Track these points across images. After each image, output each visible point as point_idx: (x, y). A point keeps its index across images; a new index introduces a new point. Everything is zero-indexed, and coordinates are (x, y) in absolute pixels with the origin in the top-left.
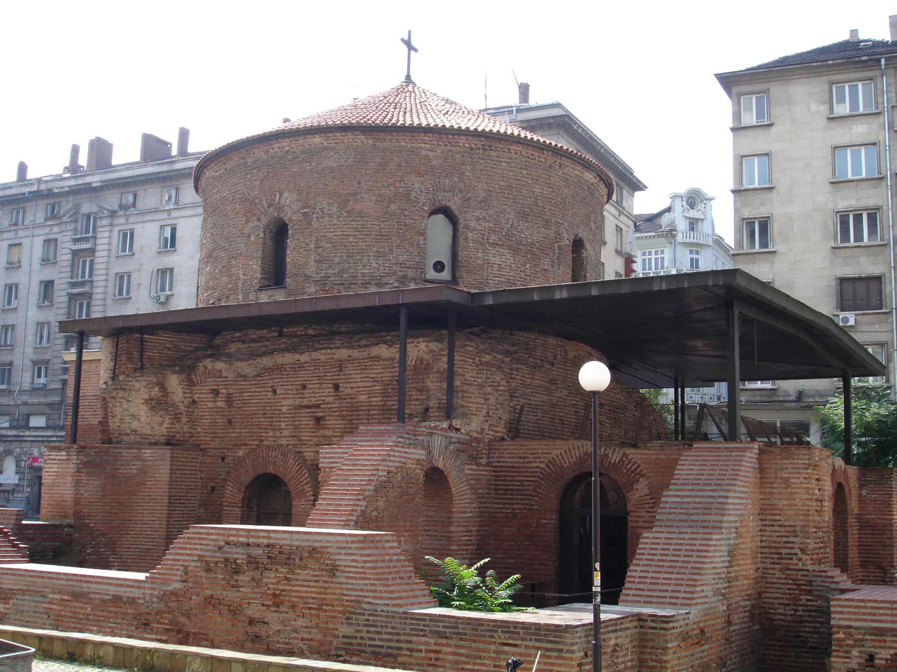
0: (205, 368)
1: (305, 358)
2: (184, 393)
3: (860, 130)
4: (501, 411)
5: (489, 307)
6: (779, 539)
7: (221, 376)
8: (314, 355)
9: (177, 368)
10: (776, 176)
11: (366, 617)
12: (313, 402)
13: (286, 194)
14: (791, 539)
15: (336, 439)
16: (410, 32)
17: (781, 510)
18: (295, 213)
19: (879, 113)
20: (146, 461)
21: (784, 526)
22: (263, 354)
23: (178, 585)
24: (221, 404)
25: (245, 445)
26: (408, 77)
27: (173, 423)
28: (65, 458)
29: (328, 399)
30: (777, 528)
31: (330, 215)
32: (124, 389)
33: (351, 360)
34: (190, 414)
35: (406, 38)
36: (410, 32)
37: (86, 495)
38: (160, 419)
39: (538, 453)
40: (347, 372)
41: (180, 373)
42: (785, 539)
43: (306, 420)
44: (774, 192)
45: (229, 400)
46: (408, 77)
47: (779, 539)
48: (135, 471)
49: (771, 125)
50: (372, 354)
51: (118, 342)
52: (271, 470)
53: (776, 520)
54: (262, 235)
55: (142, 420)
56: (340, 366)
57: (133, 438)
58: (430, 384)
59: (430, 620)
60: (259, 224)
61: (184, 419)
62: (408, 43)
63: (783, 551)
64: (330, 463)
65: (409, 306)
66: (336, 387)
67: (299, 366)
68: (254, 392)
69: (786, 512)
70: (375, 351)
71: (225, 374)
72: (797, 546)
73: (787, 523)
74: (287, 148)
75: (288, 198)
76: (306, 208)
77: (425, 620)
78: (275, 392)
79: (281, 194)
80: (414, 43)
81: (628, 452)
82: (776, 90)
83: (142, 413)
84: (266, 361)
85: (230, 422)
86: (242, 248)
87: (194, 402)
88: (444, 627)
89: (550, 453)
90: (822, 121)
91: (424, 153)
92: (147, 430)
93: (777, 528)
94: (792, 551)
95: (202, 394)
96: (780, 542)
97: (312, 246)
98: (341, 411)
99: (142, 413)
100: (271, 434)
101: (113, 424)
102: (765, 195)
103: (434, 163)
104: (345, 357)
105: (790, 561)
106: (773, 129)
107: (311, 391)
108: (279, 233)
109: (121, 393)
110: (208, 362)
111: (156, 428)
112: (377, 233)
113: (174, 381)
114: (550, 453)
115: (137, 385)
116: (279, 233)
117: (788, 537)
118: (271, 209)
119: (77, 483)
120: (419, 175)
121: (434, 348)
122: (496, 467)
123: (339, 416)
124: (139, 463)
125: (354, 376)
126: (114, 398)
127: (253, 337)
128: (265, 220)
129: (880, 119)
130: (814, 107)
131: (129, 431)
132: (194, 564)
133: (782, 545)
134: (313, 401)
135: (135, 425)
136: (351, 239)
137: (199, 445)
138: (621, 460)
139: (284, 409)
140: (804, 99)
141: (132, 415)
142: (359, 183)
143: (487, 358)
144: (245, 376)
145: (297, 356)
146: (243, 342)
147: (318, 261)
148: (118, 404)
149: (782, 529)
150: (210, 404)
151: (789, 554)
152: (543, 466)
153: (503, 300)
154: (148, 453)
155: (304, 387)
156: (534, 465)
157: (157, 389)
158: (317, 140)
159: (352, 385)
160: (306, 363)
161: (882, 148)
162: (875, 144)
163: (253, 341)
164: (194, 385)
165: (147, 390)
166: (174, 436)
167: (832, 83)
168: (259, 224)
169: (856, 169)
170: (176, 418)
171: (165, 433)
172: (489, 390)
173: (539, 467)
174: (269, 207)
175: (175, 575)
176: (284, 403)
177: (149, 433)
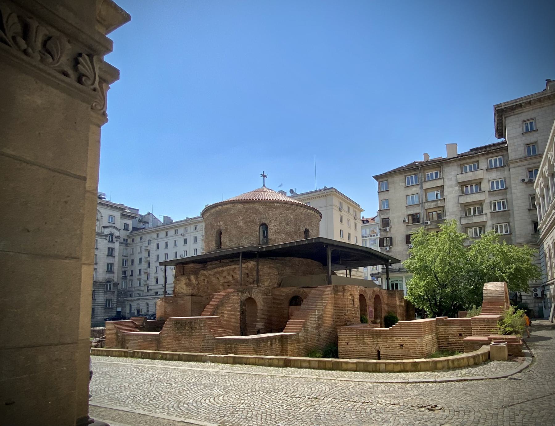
1: (224, 269)
33: (235, 268)
66: (233, 276)
67: (223, 271)
82: (390, 180)
84: (215, 270)
102: (388, 211)
129: (419, 186)
130: (401, 184)
140: (399, 181)
153: (268, 249)
167: (405, 176)
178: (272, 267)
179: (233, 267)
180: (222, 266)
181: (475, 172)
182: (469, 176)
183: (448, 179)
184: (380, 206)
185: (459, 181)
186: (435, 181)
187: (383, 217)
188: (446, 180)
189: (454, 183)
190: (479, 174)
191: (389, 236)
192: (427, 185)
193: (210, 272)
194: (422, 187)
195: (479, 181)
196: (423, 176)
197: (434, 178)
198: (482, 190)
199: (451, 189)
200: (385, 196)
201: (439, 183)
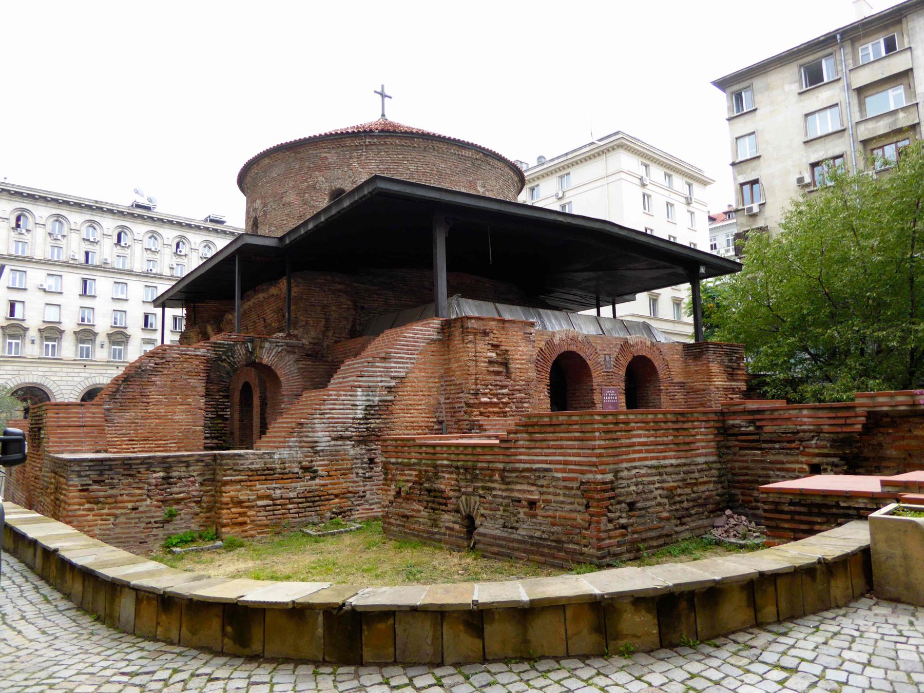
4: (345, 322)
16: (383, 86)
19: (839, 79)
26: (383, 115)
30: (452, 387)
35: (379, 90)
36: (383, 86)
41: (212, 325)
44: (761, 159)
46: (383, 115)
49: (755, 110)
62: (383, 95)
66: (265, 320)
80: (387, 92)
90: (794, 97)
91: (324, 155)
94: (460, 405)
103: (330, 160)
106: (757, 112)
120: (320, 170)
129: (841, 84)
130: (787, 87)
143: (339, 287)
161: (844, 106)
162: (837, 105)
172: (334, 308)
178: (340, 291)
186: (885, 62)
187: (742, 180)
188: (918, 52)
191: (760, 223)
192: (863, 78)
194: (849, 86)
196: (850, 56)
197: (883, 54)
200: (744, 126)
201: (897, 64)
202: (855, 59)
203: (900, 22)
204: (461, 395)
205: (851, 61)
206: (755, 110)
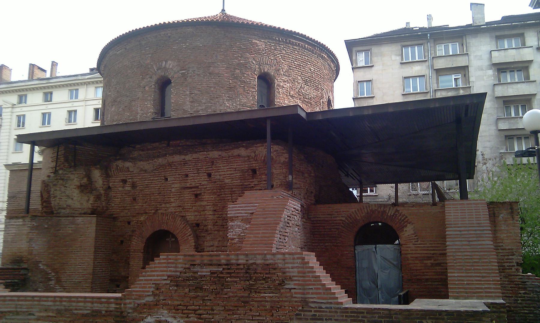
0: (117, 166)
1: (188, 157)
2: (103, 182)
3: (417, 69)
5: (320, 121)
6: (503, 257)
7: (129, 171)
8: (195, 156)
9: (98, 166)
10: (375, 91)
11: (313, 313)
12: (193, 185)
13: (169, 62)
14: (511, 257)
15: (209, 207)
17: (503, 240)
18: (175, 73)
19: (426, 61)
20: (78, 225)
21: (505, 249)
22: (159, 157)
23: (150, 299)
24: (129, 189)
25: (146, 213)
26: (223, 10)
27: (96, 201)
28: (21, 223)
29: (203, 183)
30: (500, 251)
31: (199, 75)
32: (63, 179)
34: (107, 195)
37: (36, 248)
38: (87, 198)
39: (340, 212)
40: (218, 165)
42: (506, 257)
43: (188, 195)
44: (374, 99)
45: (134, 186)
46: (223, 10)
47: (503, 257)
48: (70, 232)
49: (373, 66)
50: (235, 154)
51: (58, 150)
52: (165, 227)
53: (500, 246)
54: (153, 86)
55: (75, 199)
56: (213, 162)
57: (68, 211)
58: (274, 171)
59: (367, 313)
60: (151, 80)
61: (103, 198)
63: (506, 264)
64: (236, 213)
65: (272, 118)
66: (209, 175)
67: (185, 163)
68: (153, 180)
69: (506, 241)
70: (236, 152)
71: (131, 170)
72: (514, 261)
73: (507, 248)
74: (169, 35)
75: (170, 64)
76: (183, 70)
77: (363, 313)
78: (166, 179)
79: (166, 62)
81: (398, 209)
82: (375, 49)
83: (75, 194)
85: (135, 199)
86: (140, 95)
87: (109, 188)
88: (379, 317)
89: (348, 211)
90: (397, 65)
92: (77, 205)
93: (500, 251)
94: (511, 264)
95: (115, 182)
96: (503, 260)
97: (188, 93)
98: (213, 190)
99: (75, 194)
100: (163, 205)
101: (54, 203)
104: (217, 156)
105: (511, 270)
106: (373, 68)
107: (191, 178)
108: (164, 84)
109: (61, 182)
110: (120, 163)
111: (84, 204)
112: (228, 86)
113: (97, 174)
114: (348, 211)
115: (72, 177)
116: (164, 84)
117: (508, 256)
118: (159, 71)
119: (31, 240)
121: (277, 149)
122: (314, 221)
123: (211, 193)
124: (73, 226)
125: (222, 168)
126: (55, 185)
127: (149, 147)
128: (155, 78)
129: (427, 63)
130: (394, 57)
131: (65, 206)
132: (164, 282)
133: (505, 261)
134: (193, 184)
135: (70, 202)
136: (212, 89)
137: (113, 214)
138: (394, 214)
139: (173, 190)
141: (68, 196)
142: (216, 56)
144: (145, 171)
145: (183, 157)
146: (143, 150)
147: (192, 102)
148: (58, 189)
149: (504, 251)
150: (120, 189)
151: (510, 266)
152: (344, 219)
154: (80, 220)
155: (187, 176)
156: (338, 218)
157: (86, 179)
158: (190, 30)
159: (220, 173)
160: (189, 161)
162: (424, 76)
163: (148, 150)
164: (110, 177)
165: (79, 180)
166: (96, 209)
168: (151, 80)
169: (415, 88)
170: (98, 197)
171: (90, 207)
173: (341, 220)
174: (157, 70)
175: (148, 291)
176: (173, 186)
177: (79, 207)
179: (215, 154)
180: (180, 153)
181: (521, 50)
182: (511, 55)
183: (476, 56)
184: (356, 90)
185: (496, 61)
188: (472, 57)
189: (485, 63)
190: (527, 54)
192: (440, 64)
193: (142, 164)
194: (432, 66)
195: (526, 65)
198: (531, 79)
199: (480, 73)
201: (461, 62)
202: (435, 52)
203: (461, 37)
204: (511, 257)
205: (433, 52)
206: (373, 66)
